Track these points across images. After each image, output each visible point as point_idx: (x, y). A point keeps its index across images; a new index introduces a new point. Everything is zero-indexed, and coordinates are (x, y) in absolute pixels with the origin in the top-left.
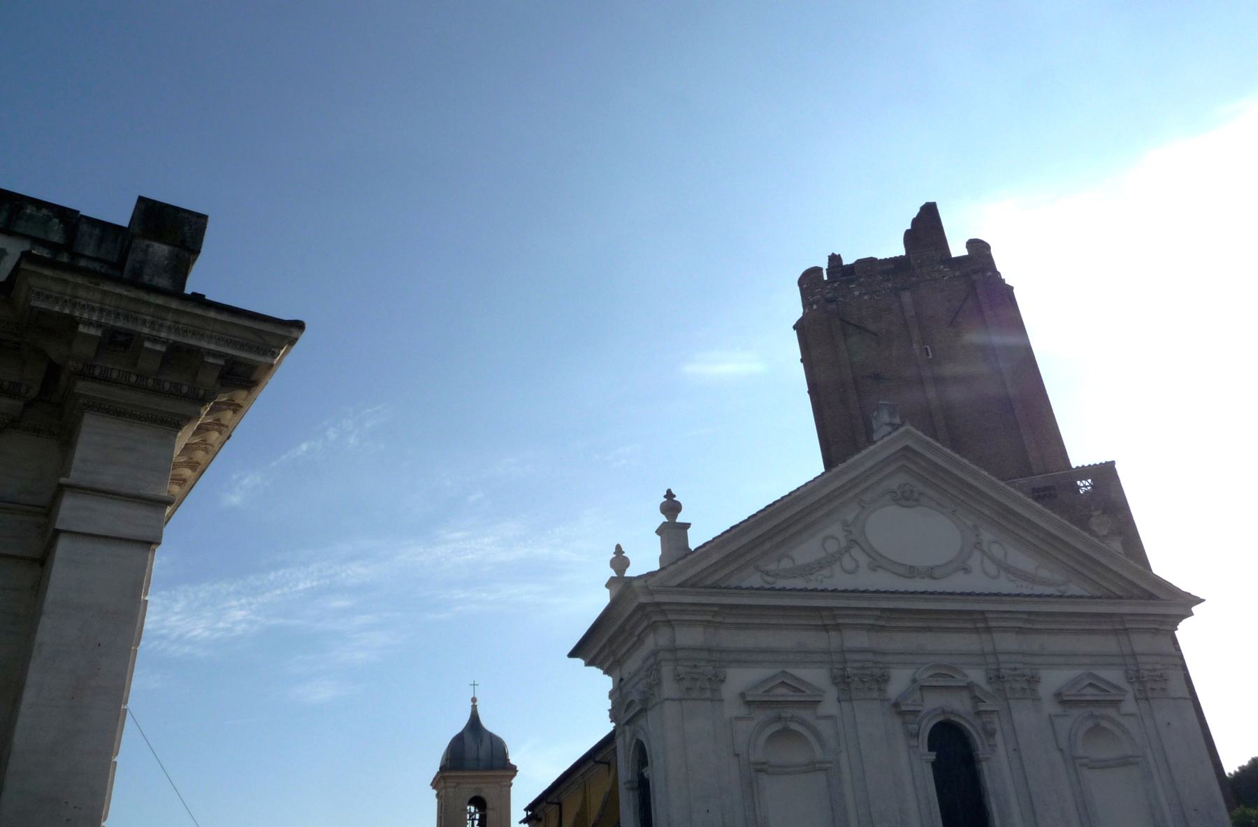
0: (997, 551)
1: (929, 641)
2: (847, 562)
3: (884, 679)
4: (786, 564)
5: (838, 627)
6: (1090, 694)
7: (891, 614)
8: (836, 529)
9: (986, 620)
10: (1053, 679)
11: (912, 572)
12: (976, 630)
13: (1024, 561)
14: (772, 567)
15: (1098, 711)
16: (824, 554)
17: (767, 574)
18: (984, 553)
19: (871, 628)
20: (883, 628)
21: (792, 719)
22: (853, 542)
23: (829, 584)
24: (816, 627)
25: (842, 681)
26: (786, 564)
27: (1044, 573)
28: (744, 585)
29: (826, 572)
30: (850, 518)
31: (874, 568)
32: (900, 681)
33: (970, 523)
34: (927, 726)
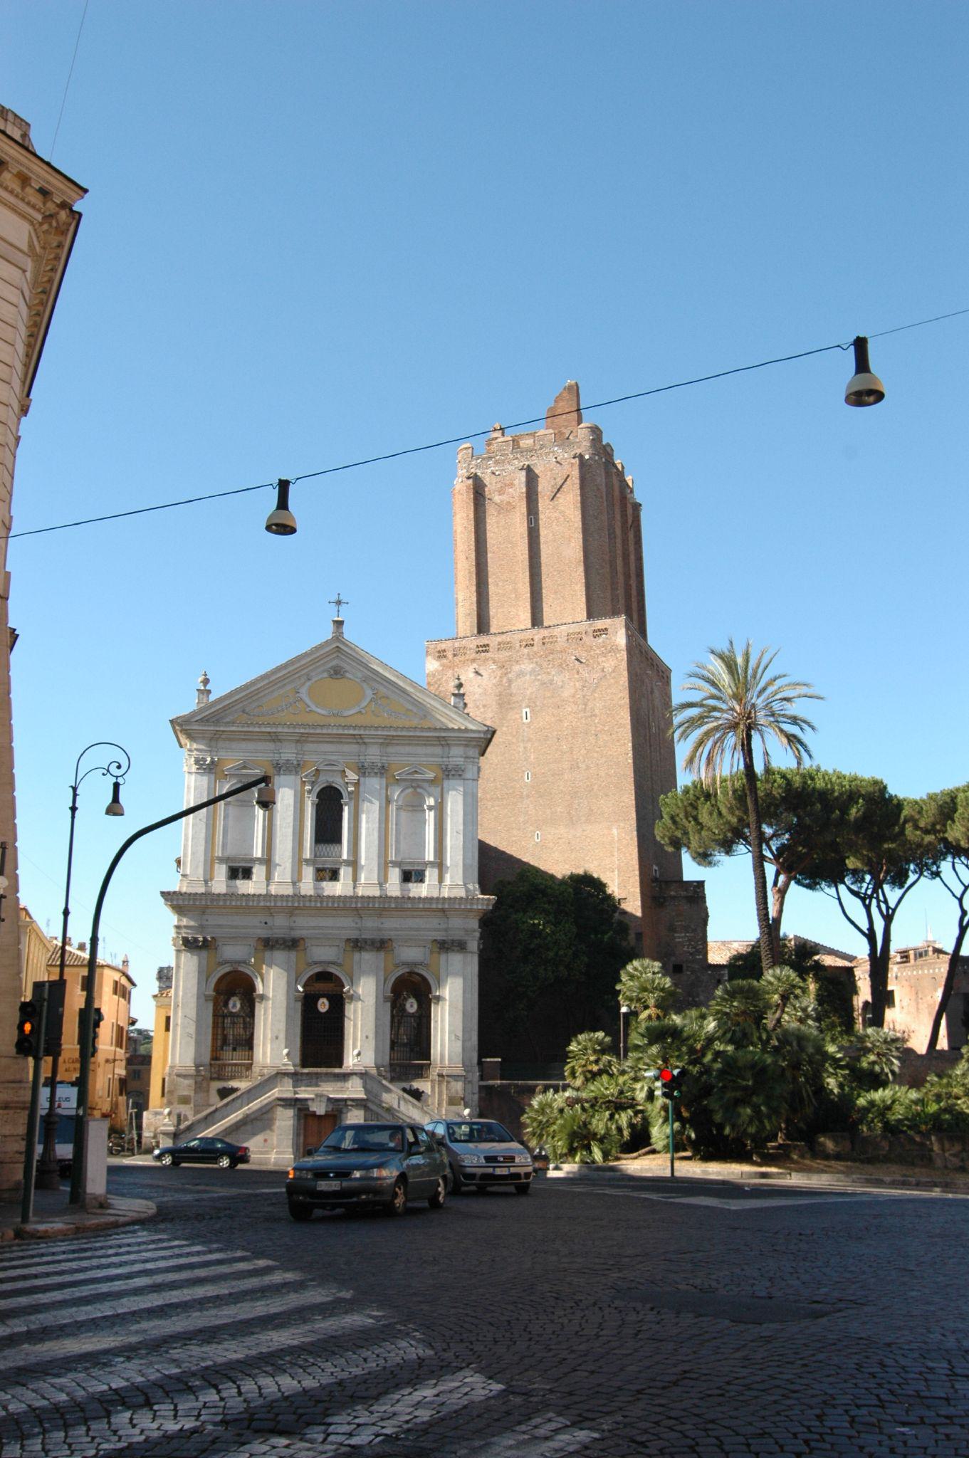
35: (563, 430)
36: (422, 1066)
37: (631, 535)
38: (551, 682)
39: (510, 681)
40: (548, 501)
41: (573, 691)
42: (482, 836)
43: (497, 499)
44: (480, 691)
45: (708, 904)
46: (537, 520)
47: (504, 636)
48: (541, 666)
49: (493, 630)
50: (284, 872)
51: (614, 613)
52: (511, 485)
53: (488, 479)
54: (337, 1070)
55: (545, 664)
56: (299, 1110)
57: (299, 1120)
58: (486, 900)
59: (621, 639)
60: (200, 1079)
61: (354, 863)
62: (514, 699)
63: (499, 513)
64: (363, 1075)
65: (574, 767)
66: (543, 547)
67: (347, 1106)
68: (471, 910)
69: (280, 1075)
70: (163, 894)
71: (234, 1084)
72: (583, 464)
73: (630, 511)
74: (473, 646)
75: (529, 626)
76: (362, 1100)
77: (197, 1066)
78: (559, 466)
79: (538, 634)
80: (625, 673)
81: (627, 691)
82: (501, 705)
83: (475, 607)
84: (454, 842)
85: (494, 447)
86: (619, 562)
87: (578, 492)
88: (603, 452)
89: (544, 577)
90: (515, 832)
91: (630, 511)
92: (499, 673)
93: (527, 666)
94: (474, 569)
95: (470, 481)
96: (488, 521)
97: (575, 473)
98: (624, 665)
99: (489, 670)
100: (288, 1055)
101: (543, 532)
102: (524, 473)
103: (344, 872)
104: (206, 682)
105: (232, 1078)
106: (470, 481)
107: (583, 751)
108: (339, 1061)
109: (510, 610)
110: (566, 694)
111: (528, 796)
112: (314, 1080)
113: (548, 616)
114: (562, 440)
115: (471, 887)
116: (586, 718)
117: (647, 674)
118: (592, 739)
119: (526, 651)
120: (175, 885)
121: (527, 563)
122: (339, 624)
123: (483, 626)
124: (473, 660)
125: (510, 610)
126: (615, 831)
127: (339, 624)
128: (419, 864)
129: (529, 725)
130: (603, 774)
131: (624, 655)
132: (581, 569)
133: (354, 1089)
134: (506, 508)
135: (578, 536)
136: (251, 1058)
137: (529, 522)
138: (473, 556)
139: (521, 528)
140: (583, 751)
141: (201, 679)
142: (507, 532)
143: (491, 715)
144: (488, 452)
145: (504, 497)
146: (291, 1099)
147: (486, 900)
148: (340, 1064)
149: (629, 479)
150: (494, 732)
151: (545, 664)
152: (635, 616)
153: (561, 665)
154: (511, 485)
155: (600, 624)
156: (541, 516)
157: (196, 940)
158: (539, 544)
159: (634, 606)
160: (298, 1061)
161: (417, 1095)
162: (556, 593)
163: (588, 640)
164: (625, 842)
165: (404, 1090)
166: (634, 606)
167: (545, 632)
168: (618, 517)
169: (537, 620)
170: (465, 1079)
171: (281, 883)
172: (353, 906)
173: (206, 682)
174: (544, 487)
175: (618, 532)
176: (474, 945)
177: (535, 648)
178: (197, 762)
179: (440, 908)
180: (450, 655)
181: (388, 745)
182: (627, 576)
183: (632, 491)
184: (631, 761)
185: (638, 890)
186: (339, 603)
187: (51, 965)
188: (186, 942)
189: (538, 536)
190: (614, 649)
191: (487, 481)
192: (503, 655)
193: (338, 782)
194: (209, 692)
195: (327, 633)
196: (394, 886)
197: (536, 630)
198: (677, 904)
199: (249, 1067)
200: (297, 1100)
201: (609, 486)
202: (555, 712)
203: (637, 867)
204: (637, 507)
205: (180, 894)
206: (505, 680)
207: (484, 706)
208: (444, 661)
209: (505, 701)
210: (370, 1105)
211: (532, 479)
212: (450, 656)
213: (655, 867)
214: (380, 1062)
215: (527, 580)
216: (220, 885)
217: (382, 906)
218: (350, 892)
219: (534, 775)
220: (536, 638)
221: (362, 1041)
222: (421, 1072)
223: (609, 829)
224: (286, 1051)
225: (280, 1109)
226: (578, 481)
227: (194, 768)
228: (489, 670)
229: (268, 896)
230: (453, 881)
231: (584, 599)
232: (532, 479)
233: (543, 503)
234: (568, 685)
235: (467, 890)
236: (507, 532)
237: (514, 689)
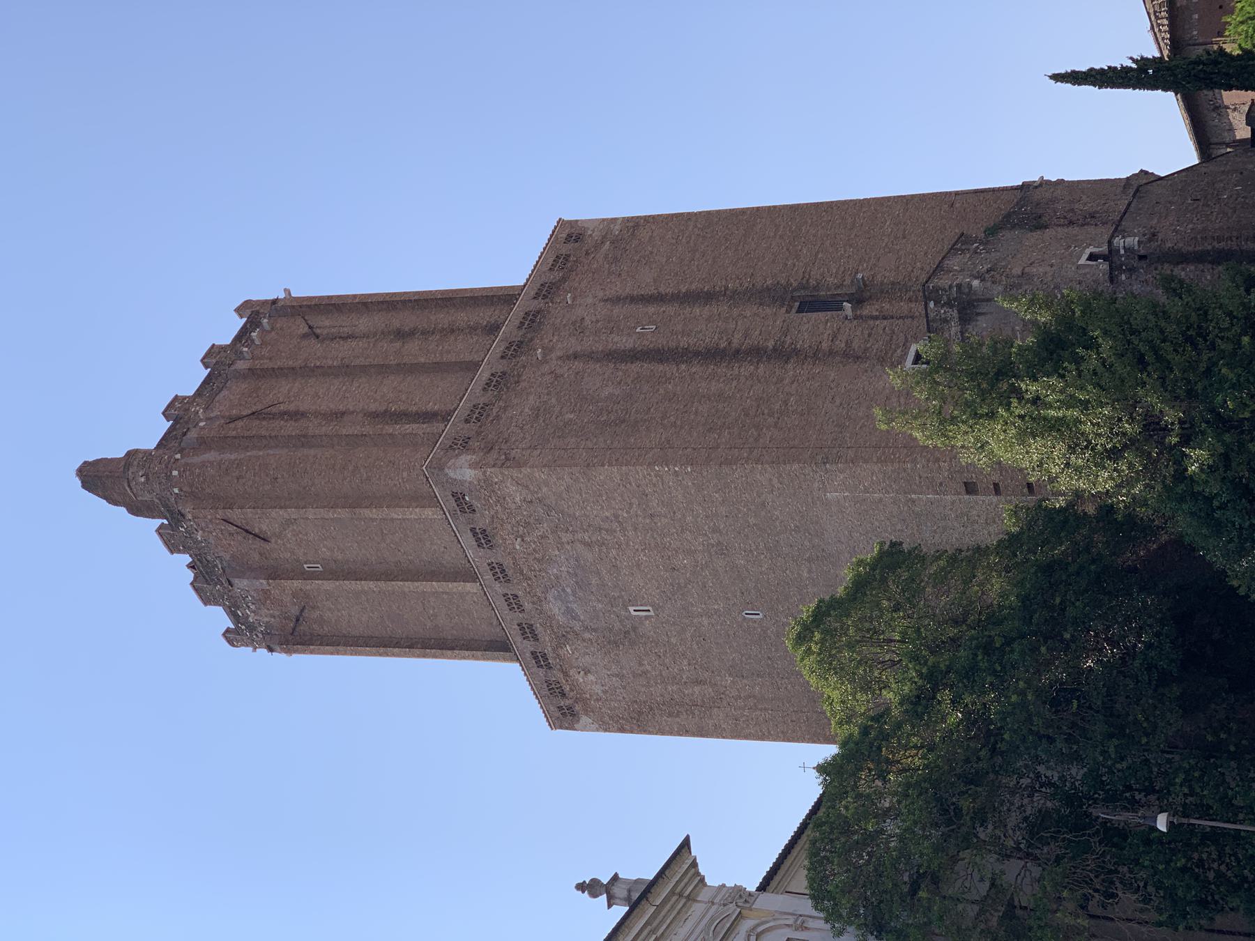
37: (324, 323)
62: (617, 625)
93: (555, 608)
119: (527, 606)
124: (566, 674)
130: (723, 510)
177: (520, 593)
206: (587, 635)
208: (577, 708)
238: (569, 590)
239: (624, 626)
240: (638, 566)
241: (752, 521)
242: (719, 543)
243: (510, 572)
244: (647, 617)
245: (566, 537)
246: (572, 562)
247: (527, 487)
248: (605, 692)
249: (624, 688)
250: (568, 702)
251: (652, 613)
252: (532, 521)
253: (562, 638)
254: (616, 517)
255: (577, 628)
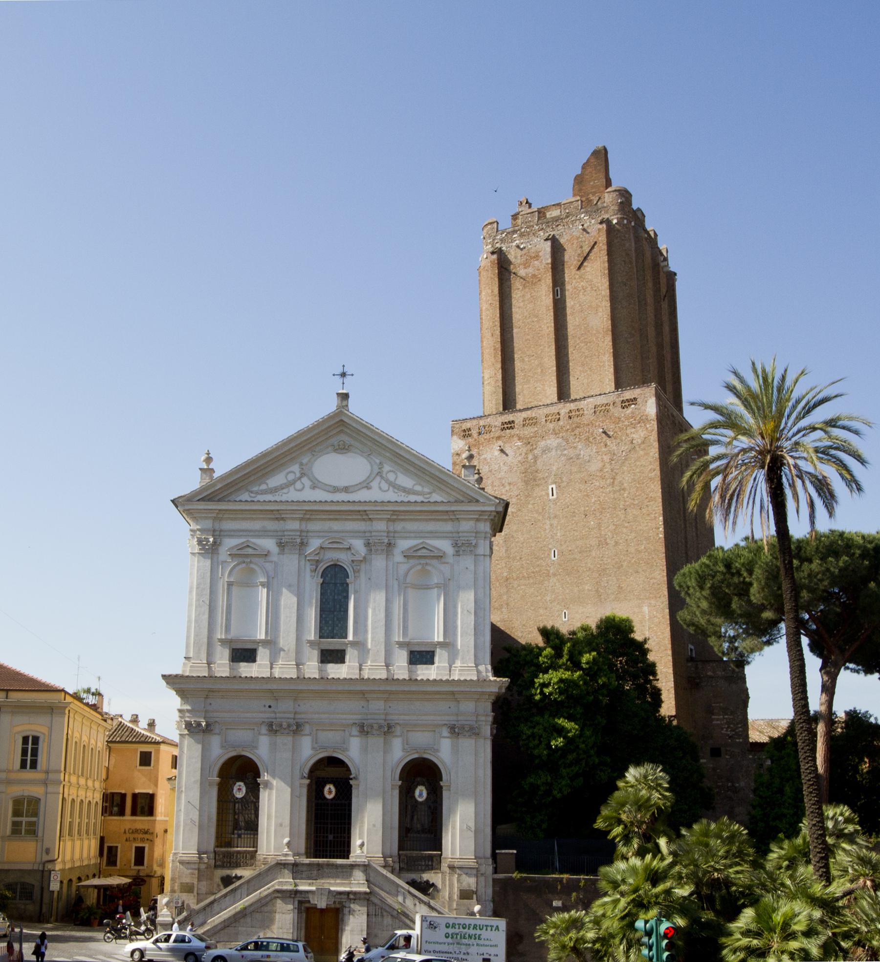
0: (391, 476)
1: (336, 526)
2: (298, 485)
3: (303, 544)
4: (263, 487)
5: (283, 519)
6: (423, 552)
7: (311, 513)
8: (296, 468)
9: (367, 515)
10: (404, 544)
11: (336, 490)
12: (364, 520)
13: (405, 481)
14: (255, 489)
15: (423, 561)
16: (285, 481)
17: (252, 492)
18: (382, 477)
19: (301, 519)
20: (309, 519)
21: (251, 562)
22: (303, 474)
23: (284, 498)
24: (270, 519)
25: (281, 545)
26: (263, 487)
27: (418, 488)
28: (237, 499)
29: (285, 491)
30: (305, 461)
31: (313, 487)
32: (315, 544)
33: (378, 461)
34: (322, 567)
35: (591, 197)
36: (431, 858)
37: (665, 305)
38: (578, 457)
39: (536, 458)
40: (574, 271)
41: (600, 465)
42: (496, 619)
43: (522, 272)
44: (505, 468)
45: (748, 685)
46: (563, 291)
47: (529, 412)
48: (567, 441)
49: (519, 407)
50: (288, 655)
51: (644, 382)
52: (537, 257)
53: (513, 255)
54: (339, 861)
55: (571, 439)
56: (300, 902)
57: (300, 912)
58: (498, 684)
59: (651, 408)
60: (203, 866)
61: (359, 645)
62: (540, 475)
63: (524, 287)
64: (366, 868)
65: (602, 543)
66: (569, 318)
67: (348, 898)
68: (483, 693)
69: (281, 865)
70: (164, 676)
71: (238, 872)
72: (611, 230)
73: (663, 281)
74: (498, 424)
75: (555, 399)
76: (366, 893)
77: (200, 853)
78: (584, 234)
79: (564, 408)
80: (656, 445)
81: (658, 463)
82: (526, 483)
83: (500, 384)
84: (465, 621)
85: (519, 221)
86: (651, 332)
87: (606, 258)
88: (633, 218)
89: (570, 350)
90: (541, 611)
91: (663, 281)
92: (524, 450)
93: (552, 441)
94: (499, 346)
95: (495, 256)
96: (514, 295)
97: (603, 239)
98: (654, 436)
99: (515, 447)
100: (289, 844)
101: (569, 303)
102: (549, 243)
103: (351, 655)
104: (209, 460)
105: (237, 865)
106: (495, 256)
107: (612, 527)
108: (344, 850)
109: (536, 384)
110: (594, 467)
111: (555, 575)
112: (317, 872)
113: (576, 388)
114: (588, 205)
115: (482, 668)
116: (615, 492)
117: (679, 449)
118: (621, 514)
119: (551, 426)
120: (177, 668)
121: (552, 336)
122: (345, 397)
123: (508, 402)
124: (498, 438)
125: (536, 384)
126: (646, 609)
127: (345, 397)
128: (427, 644)
129: (555, 502)
130: (632, 550)
131: (654, 425)
132: (608, 339)
133: (358, 883)
134: (532, 281)
135: (606, 304)
136: (255, 845)
137: (555, 293)
138: (498, 332)
139: (546, 299)
140: (612, 527)
141: (203, 458)
142: (533, 306)
143: (516, 493)
144: (514, 226)
145: (530, 270)
146: (290, 891)
147: (498, 684)
148: (346, 854)
149: (662, 246)
150: (507, 505)
151: (571, 439)
152: (669, 388)
153: (587, 439)
154: (537, 257)
155: (628, 394)
156: (568, 287)
157: (199, 724)
158: (565, 315)
159: (669, 377)
160: (302, 849)
161: (425, 888)
162: (583, 365)
163: (617, 411)
164: (656, 620)
165: (413, 883)
166: (669, 377)
167: (572, 406)
168: (650, 284)
169: (563, 394)
170: (477, 872)
171: (285, 670)
172: (360, 689)
173: (209, 460)
174: (571, 257)
175: (650, 300)
176: (487, 730)
177: (561, 423)
178: (200, 542)
179: (450, 691)
180: (474, 433)
181: (394, 521)
182: (660, 346)
183: (666, 259)
184: (662, 536)
185: (671, 671)
186: (343, 375)
187: (111, 742)
188: (188, 725)
189: (564, 308)
190: (643, 420)
191: (511, 257)
192: (529, 431)
193: (344, 558)
194: (212, 470)
195: (331, 406)
196: (401, 668)
197: (561, 405)
198: (715, 681)
199: (253, 855)
200: (297, 892)
201: (639, 252)
202: (582, 487)
203: (670, 646)
204: (672, 276)
205: (182, 677)
206: (530, 457)
207: (510, 484)
208: (470, 439)
209: (531, 477)
210: (373, 899)
211: (557, 249)
212: (475, 435)
213: (690, 646)
214: (388, 852)
215: (553, 352)
216: (222, 666)
217: (390, 689)
218: (355, 675)
219: (562, 553)
220: (563, 412)
221: (371, 830)
222: (433, 863)
223: (640, 607)
224: (286, 840)
225: (279, 901)
226: (605, 247)
227: (197, 549)
228: (515, 447)
229: (271, 679)
230: (466, 664)
231: (612, 370)
232: (557, 249)
233: (570, 273)
234: (594, 458)
235: (479, 672)
236: (533, 306)
237: (540, 464)
238: (565, 452)
239: (540, 479)
240: (587, 496)
241: (625, 564)
242: (607, 544)
243: (576, 420)
244: (548, 494)
245: (606, 458)
246: (587, 458)
247: (643, 443)
248: (485, 459)
249: (491, 471)
250: (475, 435)
251: (551, 497)
252: (618, 441)
253: (528, 442)
254: (624, 489)
255: (536, 452)
